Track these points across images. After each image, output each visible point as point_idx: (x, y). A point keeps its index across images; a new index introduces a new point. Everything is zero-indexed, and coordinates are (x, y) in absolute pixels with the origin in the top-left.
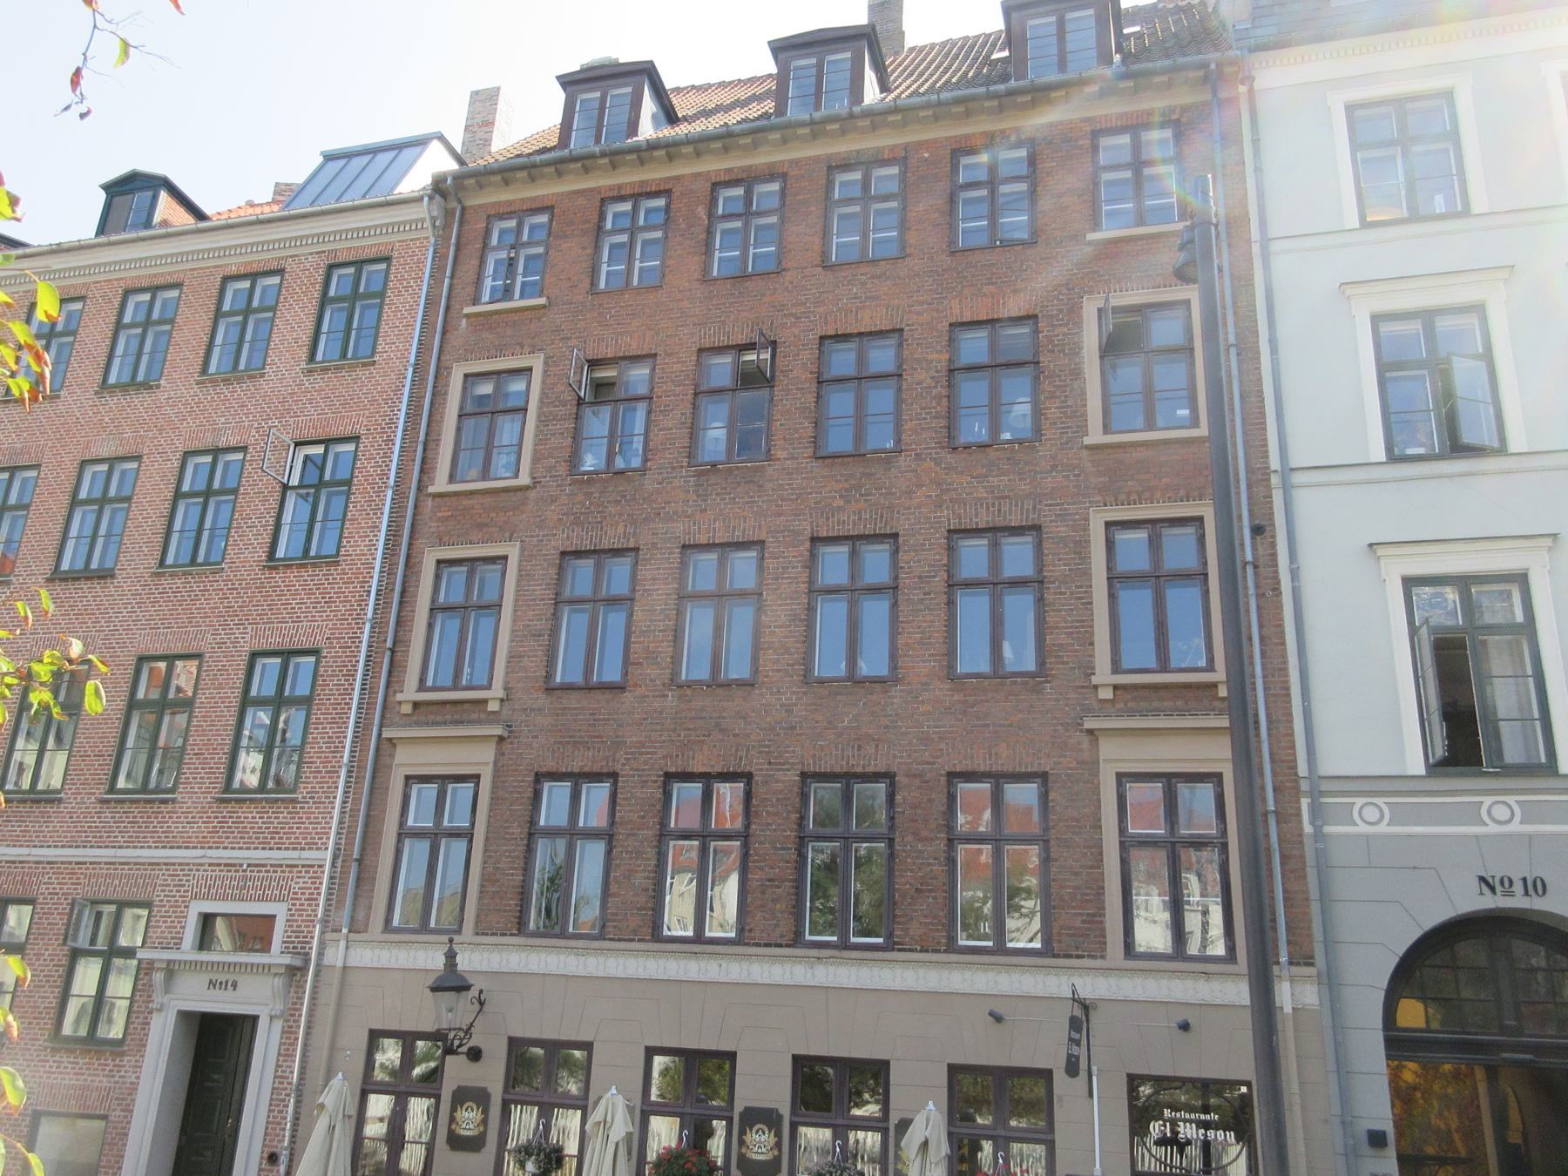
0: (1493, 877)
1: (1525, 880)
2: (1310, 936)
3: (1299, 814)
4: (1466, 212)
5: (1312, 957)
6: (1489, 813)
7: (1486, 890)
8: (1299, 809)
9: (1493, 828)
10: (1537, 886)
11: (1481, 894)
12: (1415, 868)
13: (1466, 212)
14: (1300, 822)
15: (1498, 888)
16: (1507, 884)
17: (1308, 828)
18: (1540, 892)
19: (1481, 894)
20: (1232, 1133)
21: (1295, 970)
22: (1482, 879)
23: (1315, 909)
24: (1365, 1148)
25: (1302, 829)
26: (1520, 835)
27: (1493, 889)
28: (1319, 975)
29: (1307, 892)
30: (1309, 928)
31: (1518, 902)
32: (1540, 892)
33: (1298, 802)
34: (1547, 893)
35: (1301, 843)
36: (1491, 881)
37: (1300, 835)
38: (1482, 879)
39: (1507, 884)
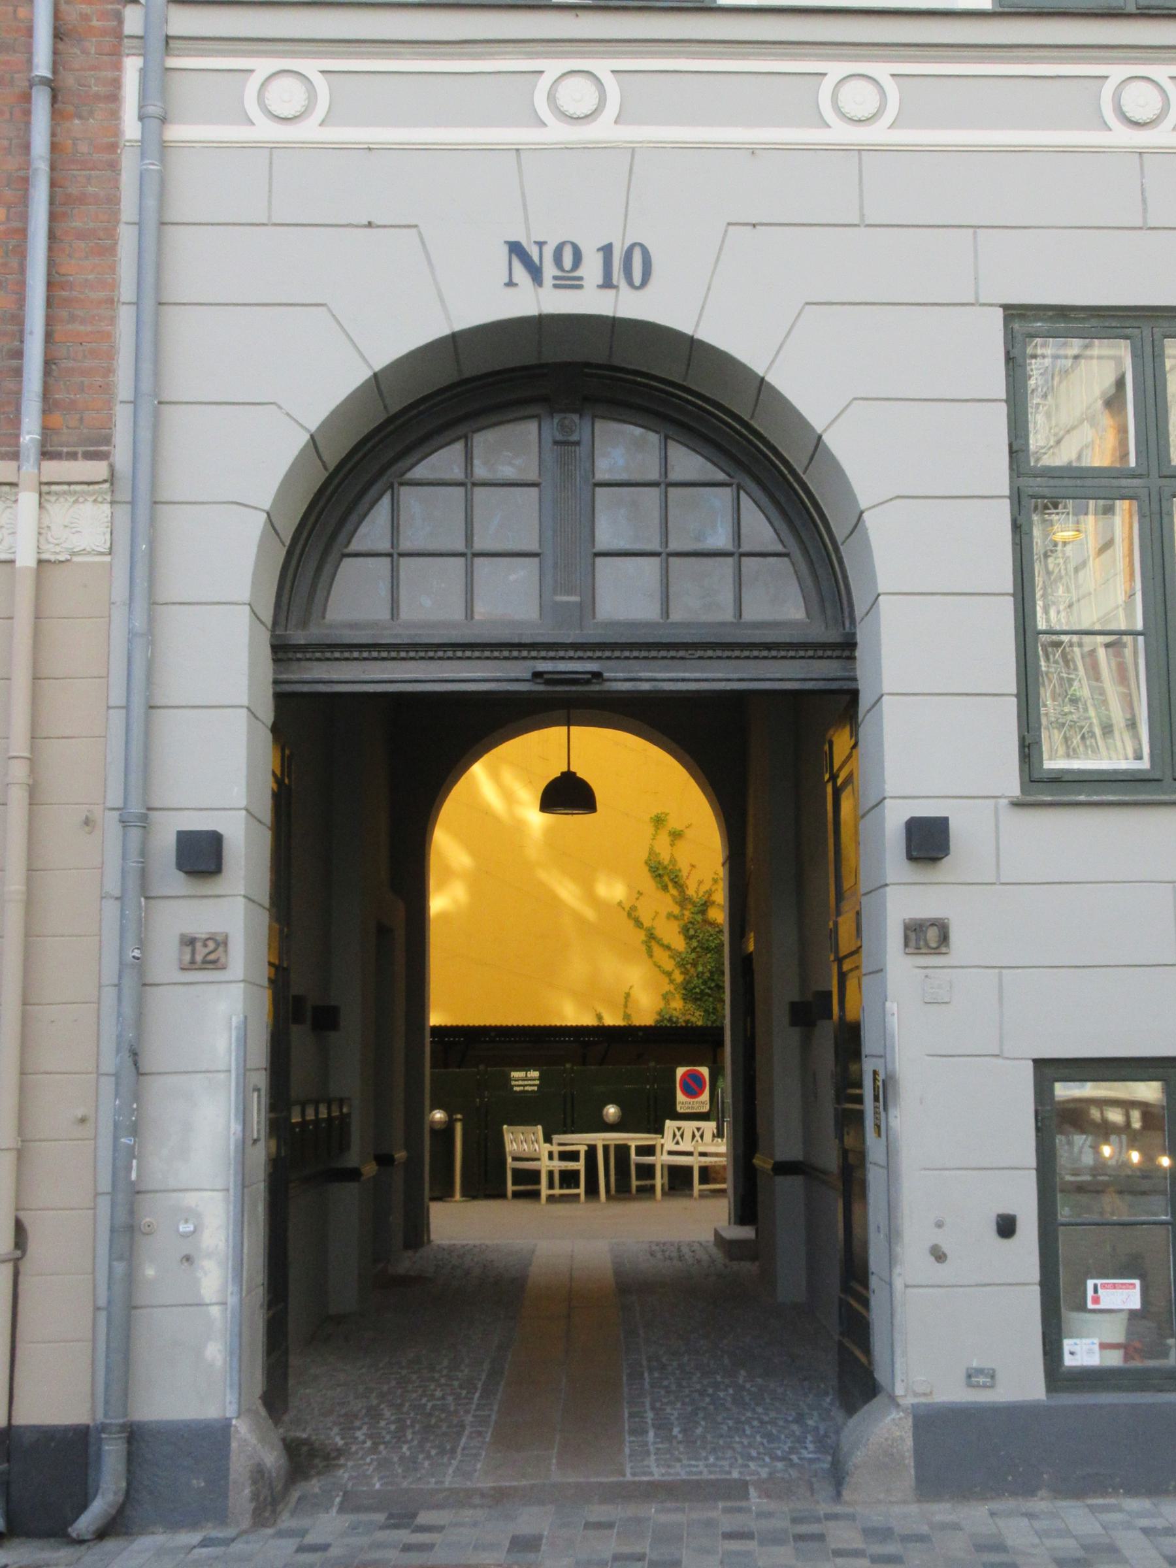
0: (541, 244)
1: (607, 250)
2: (107, 389)
3: (114, 97)
5: (107, 440)
6: (551, 97)
7: (521, 274)
8: (117, 83)
9: (557, 132)
11: (510, 284)
12: (370, 225)
14: (115, 115)
15: (549, 271)
16: (568, 261)
17: (131, 128)
18: (637, 278)
19: (510, 284)
21: (55, 469)
22: (516, 249)
23: (125, 318)
24: (171, 880)
27: (535, 273)
28: (112, 479)
29: (114, 286)
30: (109, 371)
32: (637, 278)
33: (118, 67)
35: (114, 166)
36: (534, 253)
37: (113, 147)
38: (516, 249)
39: (568, 261)
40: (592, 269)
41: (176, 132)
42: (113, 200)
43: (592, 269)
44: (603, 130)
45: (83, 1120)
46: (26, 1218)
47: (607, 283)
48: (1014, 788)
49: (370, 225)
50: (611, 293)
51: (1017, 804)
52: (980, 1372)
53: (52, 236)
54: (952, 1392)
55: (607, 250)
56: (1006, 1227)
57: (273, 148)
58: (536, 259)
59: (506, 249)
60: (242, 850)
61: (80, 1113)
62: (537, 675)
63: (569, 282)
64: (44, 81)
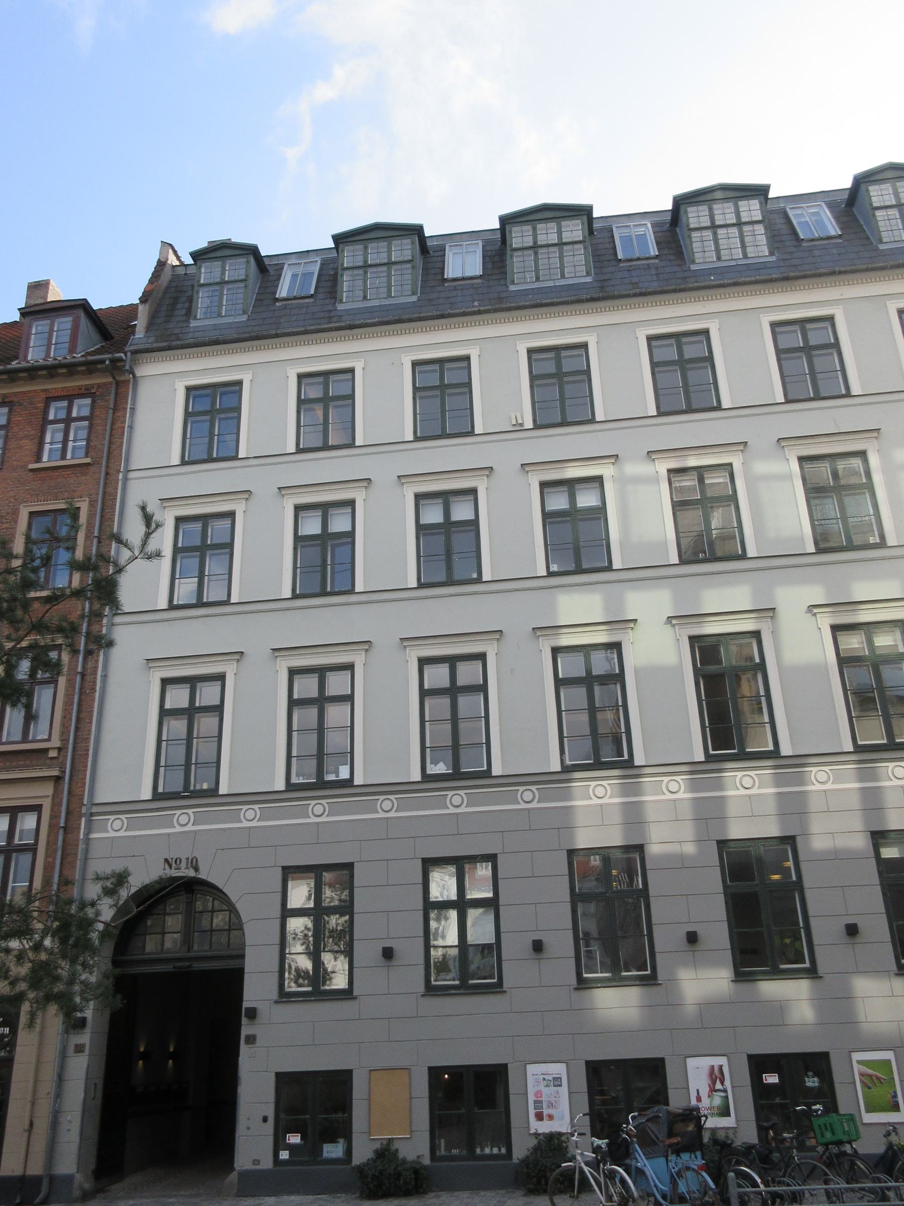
0: (172, 858)
3: (79, 828)
4: (351, 445)
7: (167, 866)
8: (80, 824)
9: (179, 829)
12: (133, 856)
13: (351, 445)
14: (79, 832)
15: (174, 865)
16: (178, 863)
20: (8, 1029)
22: (166, 860)
25: (79, 837)
26: (192, 831)
33: (80, 820)
35: (77, 845)
36: (170, 861)
37: (78, 840)
38: (166, 860)
40: (183, 864)
41: (93, 836)
42: (76, 854)
43: (183, 864)
44: (190, 828)
45: (48, 1093)
46: (33, 1119)
47: (187, 868)
48: (275, 995)
49: (133, 856)
53: (62, 864)
54: (249, 1166)
55: (187, 859)
56: (265, 1119)
57: (113, 838)
58: (166, 864)
60: (91, 1021)
61: (48, 1091)
62: (174, 967)
64: (62, 827)
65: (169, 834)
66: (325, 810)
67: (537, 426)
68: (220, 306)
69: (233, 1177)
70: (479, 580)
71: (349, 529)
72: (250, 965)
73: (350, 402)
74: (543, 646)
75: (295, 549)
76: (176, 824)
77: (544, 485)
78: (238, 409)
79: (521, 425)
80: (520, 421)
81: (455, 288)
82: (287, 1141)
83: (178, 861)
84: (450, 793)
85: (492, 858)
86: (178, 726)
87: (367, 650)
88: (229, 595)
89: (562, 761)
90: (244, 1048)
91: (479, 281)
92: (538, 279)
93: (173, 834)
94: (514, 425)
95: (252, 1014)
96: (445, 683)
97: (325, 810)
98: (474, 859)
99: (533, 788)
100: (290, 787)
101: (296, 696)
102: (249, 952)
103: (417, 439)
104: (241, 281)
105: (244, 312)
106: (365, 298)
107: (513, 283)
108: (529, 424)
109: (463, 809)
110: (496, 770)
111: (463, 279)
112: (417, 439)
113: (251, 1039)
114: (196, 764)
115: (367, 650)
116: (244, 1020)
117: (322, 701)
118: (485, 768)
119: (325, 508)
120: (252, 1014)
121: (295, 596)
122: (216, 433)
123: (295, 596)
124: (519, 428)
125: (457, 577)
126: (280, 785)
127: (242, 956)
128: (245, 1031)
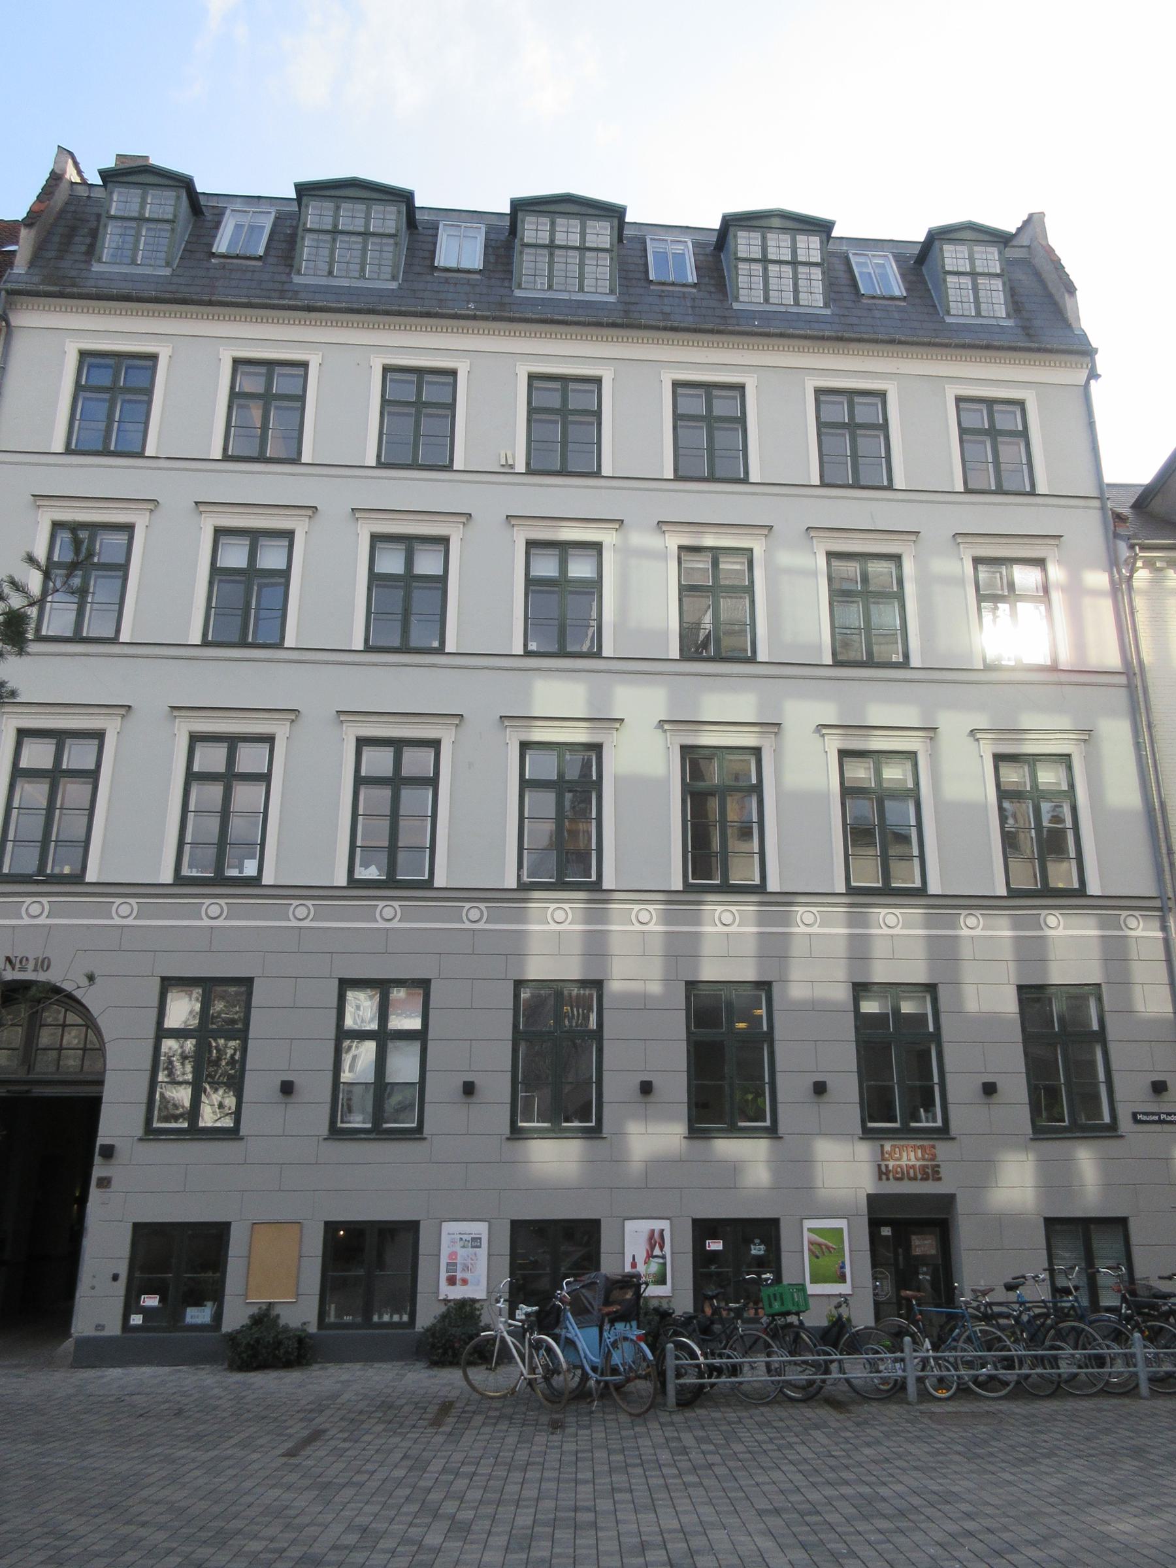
7: (8, 967)
9: (27, 921)
10: (44, 964)
15: (18, 966)
22: (8, 959)
26: (44, 925)
31: (29, 976)
34: (50, 970)
36: (14, 960)
38: (8, 959)
40: (31, 966)
44: (42, 921)
47: (35, 970)
48: (140, 1132)
50: (35, 973)
51: (141, 1139)
52: (99, 1325)
55: (36, 959)
56: (115, 1278)
59: (4, 959)
62: (8, 1091)
63: (23, 969)
65: (14, 927)
66: (222, 912)
67: (530, 472)
68: (135, 249)
69: (69, 1344)
70: (440, 651)
71: (283, 566)
72: (110, 1093)
73: (298, 404)
74: (510, 739)
75: (211, 583)
76: (24, 915)
77: (531, 544)
78: (149, 392)
79: (512, 466)
80: (510, 462)
81: (447, 281)
82: (142, 1303)
83: (24, 960)
84: (381, 904)
85: (424, 984)
86: (35, 793)
87: (293, 721)
88: (118, 631)
89: (519, 876)
90: (94, 1193)
91: (478, 277)
92: (550, 287)
93: (19, 926)
94: (503, 466)
95: (108, 1152)
96: (387, 770)
97: (222, 912)
98: (400, 983)
99: (482, 906)
100: (180, 880)
101: (196, 769)
102: (110, 1079)
103: (380, 465)
104: (167, 221)
105: (168, 264)
106: (330, 273)
107: (519, 286)
108: (521, 467)
109: (395, 924)
110: (439, 882)
111: (458, 271)
112: (380, 465)
113: (104, 1183)
114: (56, 841)
115: (293, 721)
116: (97, 1159)
117: (229, 777)
118: (426, 877)
119: (254, 536)
120: (108, 1152)
121: (206, 643)
122: (117, 419)
123: (206, 643)
124: (508, 470)
125: (414, 642)
126: (167, 877)
127: (101, 1083)
128: (98, 1171)
